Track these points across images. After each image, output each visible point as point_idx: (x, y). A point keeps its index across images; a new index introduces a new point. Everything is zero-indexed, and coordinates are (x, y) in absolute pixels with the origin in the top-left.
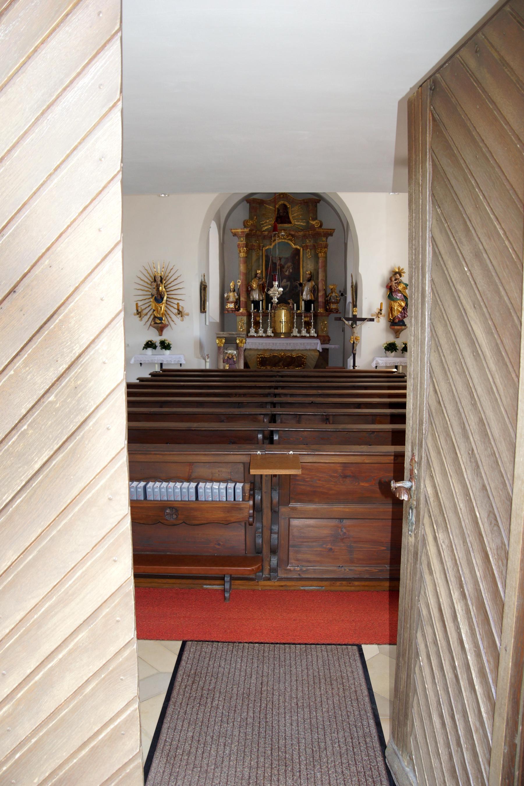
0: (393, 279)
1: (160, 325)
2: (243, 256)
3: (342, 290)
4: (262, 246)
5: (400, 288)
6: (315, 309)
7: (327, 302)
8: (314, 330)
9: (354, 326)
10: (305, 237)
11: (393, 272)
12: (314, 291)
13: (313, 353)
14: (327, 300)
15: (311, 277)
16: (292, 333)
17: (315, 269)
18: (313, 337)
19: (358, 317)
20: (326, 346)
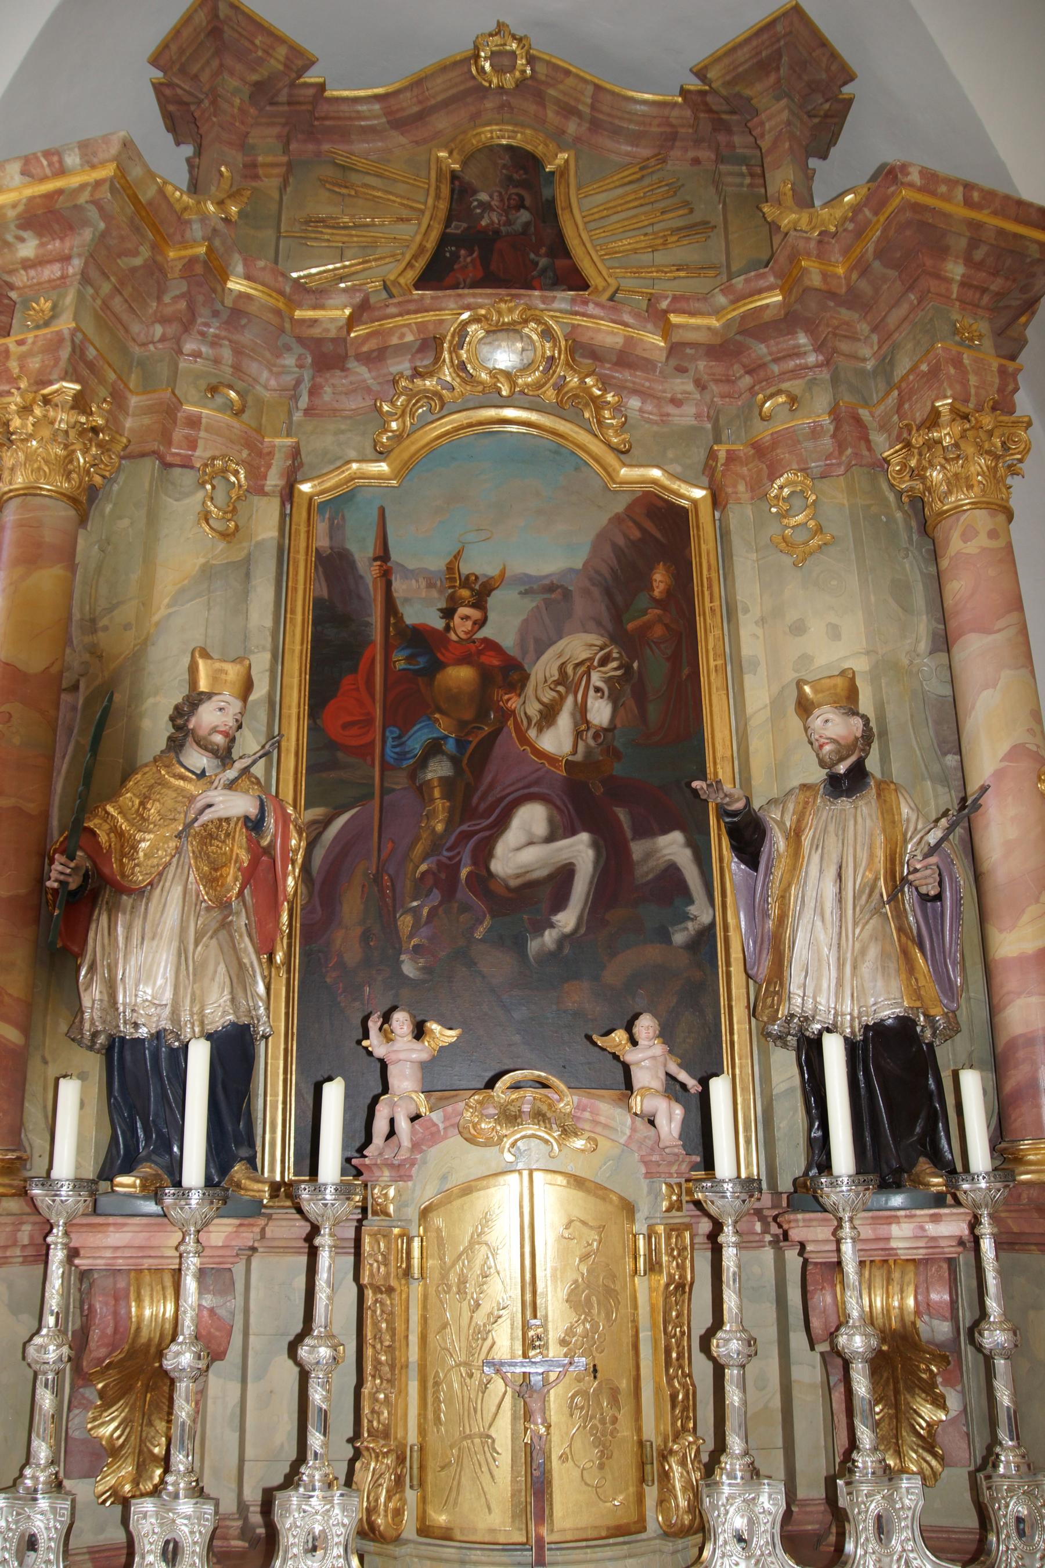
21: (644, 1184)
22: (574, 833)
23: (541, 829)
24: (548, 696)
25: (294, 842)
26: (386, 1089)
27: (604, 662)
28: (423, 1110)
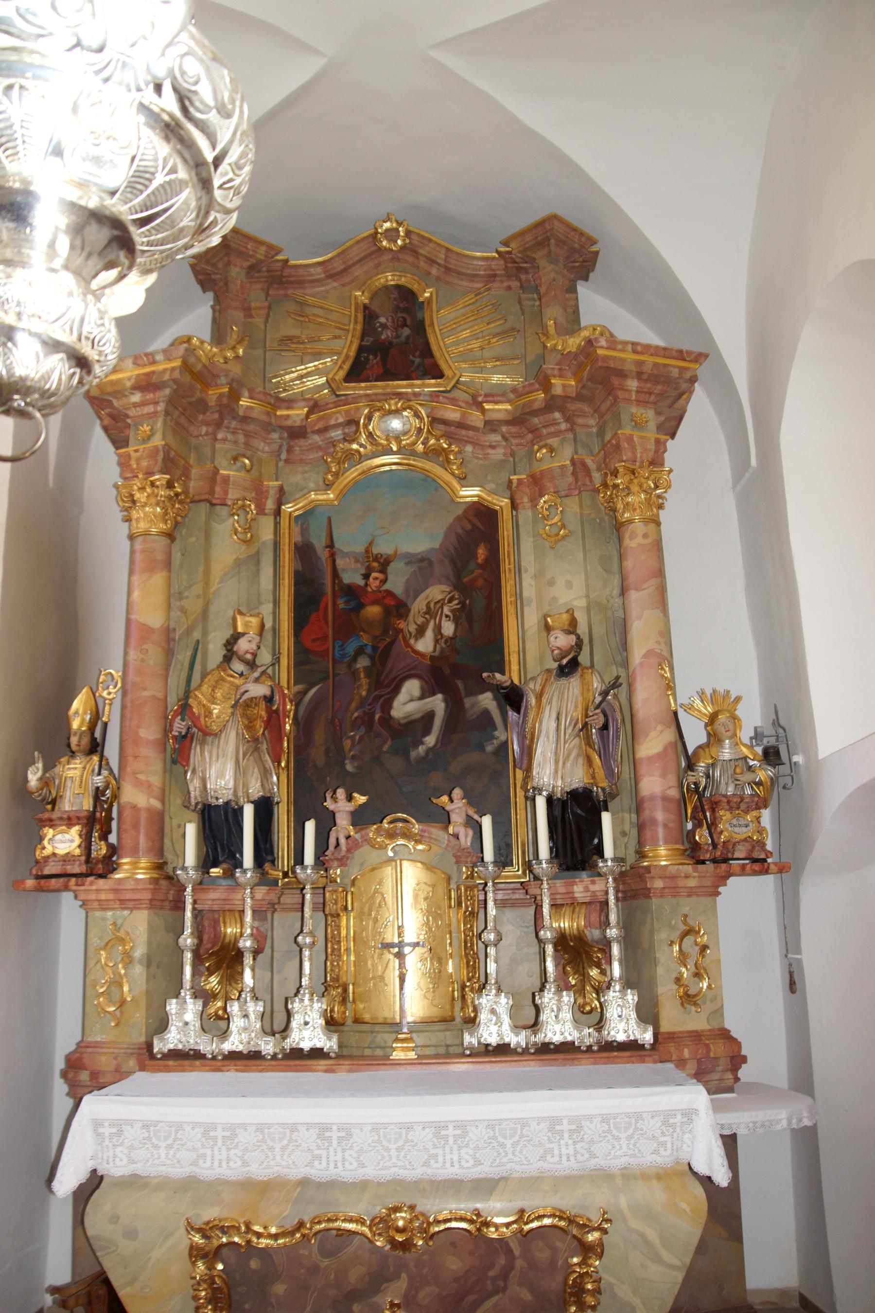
4: (272, 492)
8: (632, 997)
16: (472, 1022)
21: (455, 867)
22: (434, 694)
23: (417, 692)
24: (420, 620)
25: (288, 707)
26: (335, 825)
27: (450, 601)
28: (352, 833)
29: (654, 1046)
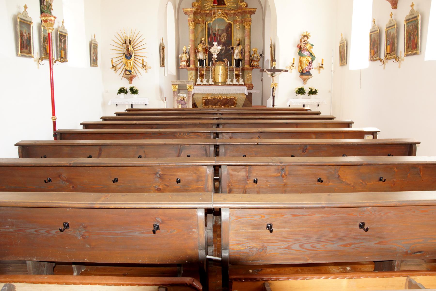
0: (303, 40)
1: (130, 76)
2: (192, 28)
3: (261, 52)
4: (205, 21)
5: (308, 47)
6: (243, 65)
7: (251, 61)
8: (242, 80)
9: (274, 75)
10: (235, 14)
11: (302, 35)
12: (242, 52)
13: (242, 96)
14: (251, 59)
15: (240, 43)
17: (242, 38)
18: (242, 85)
19: (276, 69)
20: (251, 91)
22: (224, 46)
24: (222, 37)
29: (244, 85)
